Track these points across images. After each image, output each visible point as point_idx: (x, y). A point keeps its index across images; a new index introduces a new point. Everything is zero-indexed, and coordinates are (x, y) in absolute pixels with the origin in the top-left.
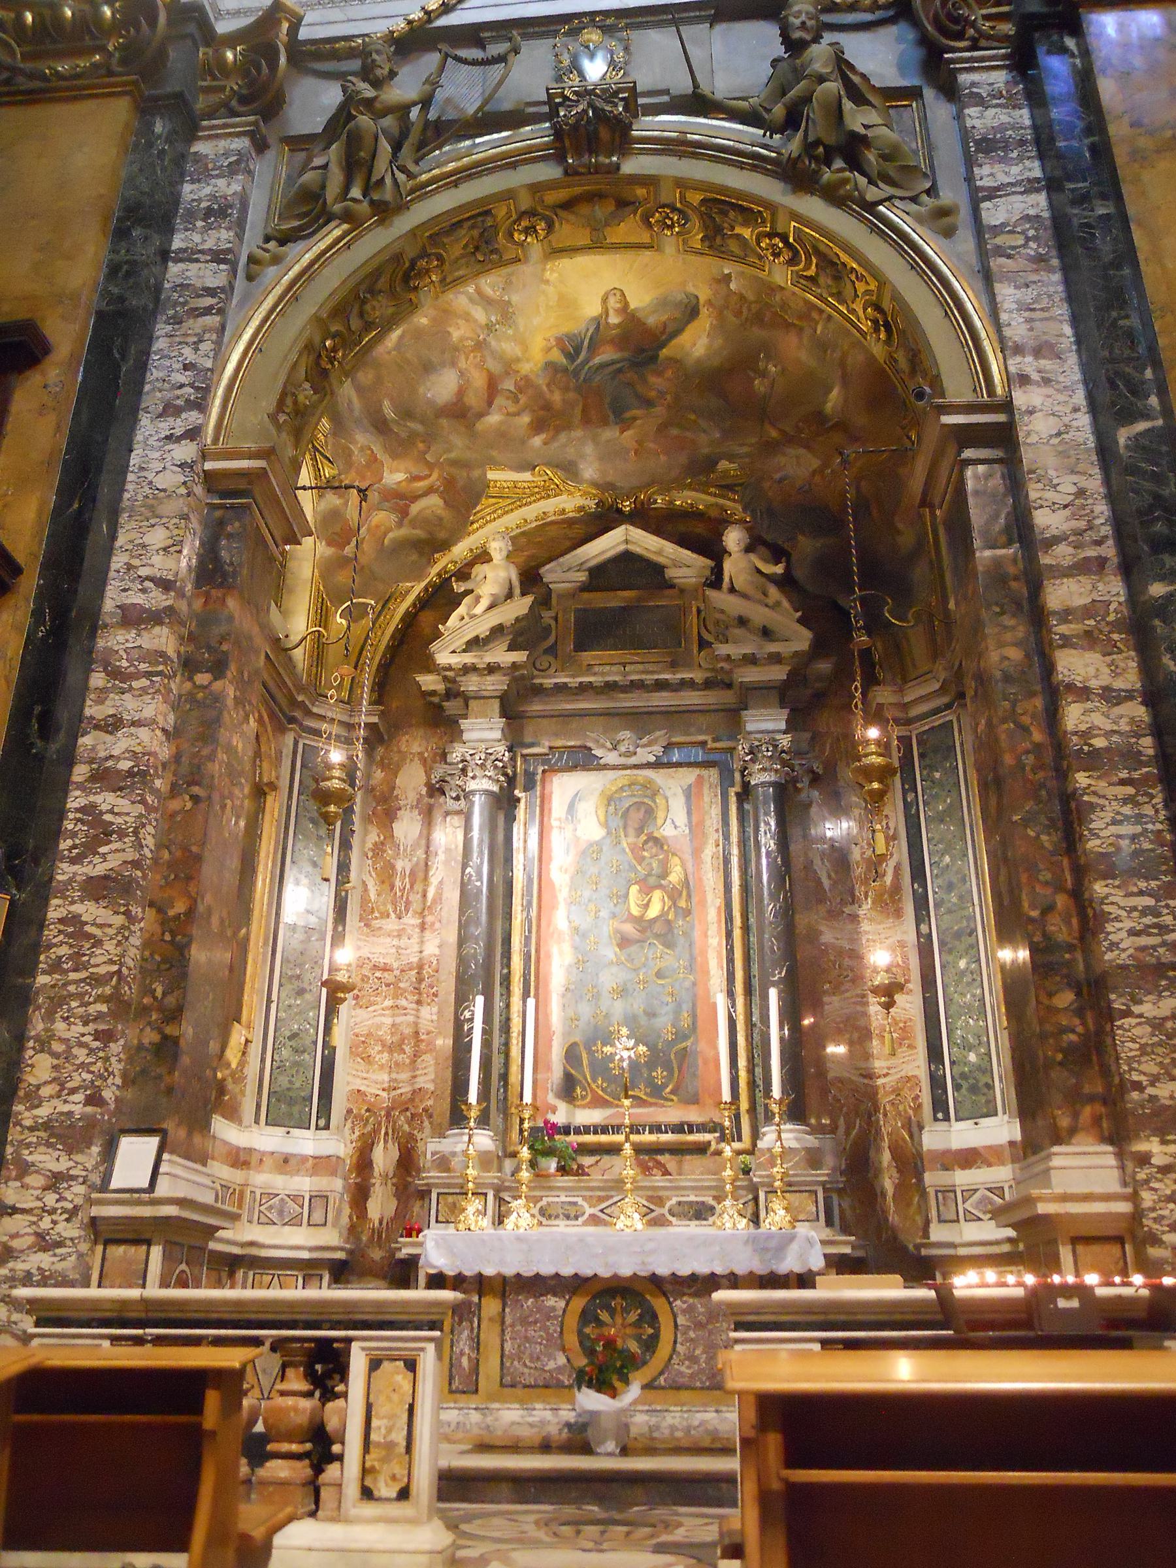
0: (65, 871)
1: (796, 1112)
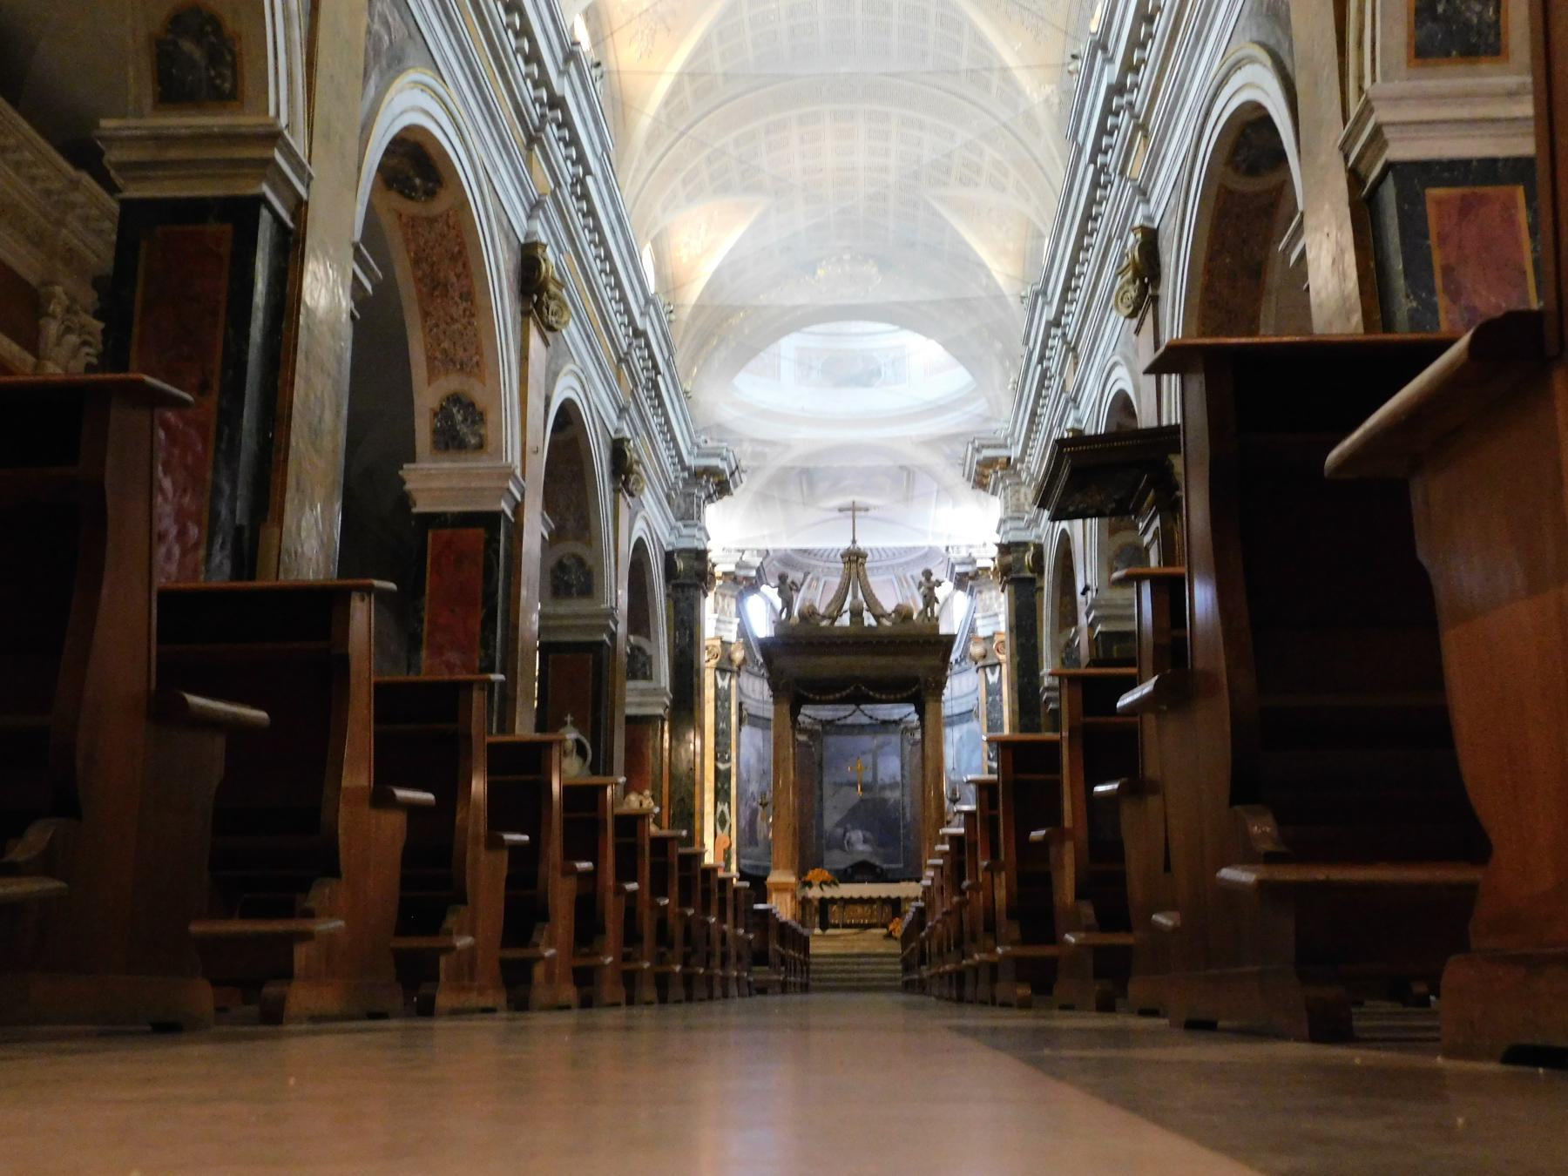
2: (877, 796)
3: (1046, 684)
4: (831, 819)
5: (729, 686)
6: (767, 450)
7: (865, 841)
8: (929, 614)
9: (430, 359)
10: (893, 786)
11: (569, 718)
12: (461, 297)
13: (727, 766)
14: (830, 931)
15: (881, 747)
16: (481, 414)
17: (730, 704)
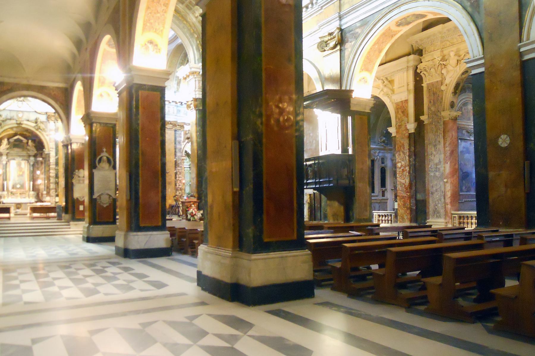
1: (33, 190)
9: (145, 25)
11: (105, 150)
12: (164, 5)
16: (159, 49)
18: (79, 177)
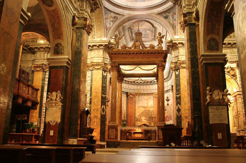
0: (42, 117)
2: (148, 109)
3: (201, 54)
4: (137, 115)
5: (107, 75)
6: (118, 16)
7: (145, 120)
8: (160, 46)
10: (151, 107)
13: (105, 96)
14: (129, 141)
15: (149, 98)
17: (107, 80)
18: (52, 100)
